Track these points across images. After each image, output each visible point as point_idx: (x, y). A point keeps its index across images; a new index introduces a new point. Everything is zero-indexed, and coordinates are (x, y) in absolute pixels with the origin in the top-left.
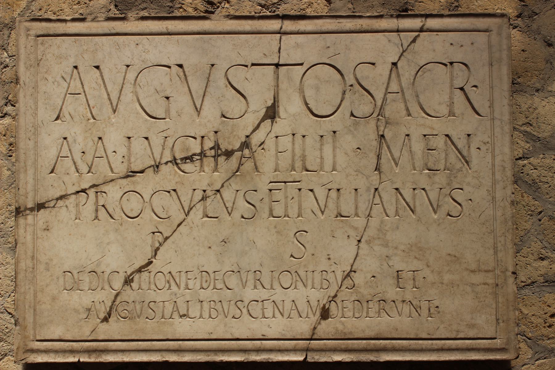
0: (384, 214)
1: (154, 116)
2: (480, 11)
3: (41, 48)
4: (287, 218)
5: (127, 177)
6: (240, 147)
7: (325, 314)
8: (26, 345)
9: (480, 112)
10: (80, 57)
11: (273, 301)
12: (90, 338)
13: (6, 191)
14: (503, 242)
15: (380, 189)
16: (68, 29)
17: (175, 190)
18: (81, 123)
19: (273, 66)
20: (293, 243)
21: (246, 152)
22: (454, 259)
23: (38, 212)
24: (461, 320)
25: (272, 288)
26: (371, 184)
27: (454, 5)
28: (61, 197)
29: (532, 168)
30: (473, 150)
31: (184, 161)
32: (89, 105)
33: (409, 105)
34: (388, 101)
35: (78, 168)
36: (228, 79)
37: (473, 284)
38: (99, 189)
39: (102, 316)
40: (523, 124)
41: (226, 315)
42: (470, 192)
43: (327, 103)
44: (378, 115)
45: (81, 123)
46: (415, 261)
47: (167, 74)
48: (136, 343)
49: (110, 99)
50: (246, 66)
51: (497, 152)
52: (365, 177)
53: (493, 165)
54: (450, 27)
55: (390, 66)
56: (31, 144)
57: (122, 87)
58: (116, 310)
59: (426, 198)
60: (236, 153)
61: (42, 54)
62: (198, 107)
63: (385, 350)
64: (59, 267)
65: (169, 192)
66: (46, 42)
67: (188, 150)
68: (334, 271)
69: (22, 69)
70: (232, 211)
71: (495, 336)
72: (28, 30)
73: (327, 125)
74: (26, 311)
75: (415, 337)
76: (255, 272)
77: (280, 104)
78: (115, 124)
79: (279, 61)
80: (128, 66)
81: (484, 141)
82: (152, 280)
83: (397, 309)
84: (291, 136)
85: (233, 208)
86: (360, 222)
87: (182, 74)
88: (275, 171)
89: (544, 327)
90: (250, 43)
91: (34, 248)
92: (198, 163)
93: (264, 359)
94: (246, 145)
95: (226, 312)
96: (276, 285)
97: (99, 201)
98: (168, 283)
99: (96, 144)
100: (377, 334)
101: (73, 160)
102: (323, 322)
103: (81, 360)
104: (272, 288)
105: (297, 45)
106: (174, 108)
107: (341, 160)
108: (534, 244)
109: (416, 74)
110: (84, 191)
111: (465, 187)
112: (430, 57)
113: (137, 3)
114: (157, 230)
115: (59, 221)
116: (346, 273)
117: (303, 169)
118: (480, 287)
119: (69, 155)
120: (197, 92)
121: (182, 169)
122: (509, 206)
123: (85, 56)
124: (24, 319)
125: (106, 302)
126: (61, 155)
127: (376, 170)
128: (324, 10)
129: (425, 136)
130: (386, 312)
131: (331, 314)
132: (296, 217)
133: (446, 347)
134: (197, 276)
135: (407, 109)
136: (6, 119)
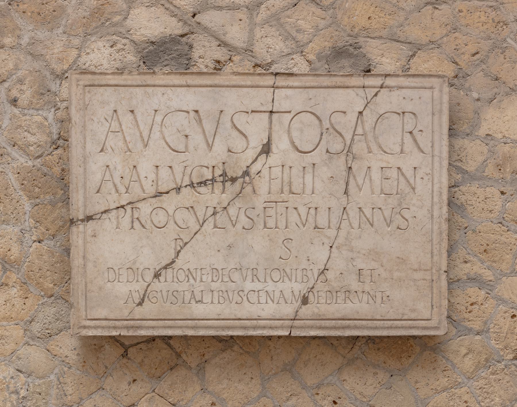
0: (350, 227)
1: (177, 150)
2: (426, 72)
3: (88, 96)
4: (277, 230)
5: (155, 196)
7: (305, 301)
9: (424, 151)
10: (119, 103)
11: (266, 291)
12: (128, 318)
14: (438, 249)
15: (347, 209)
17: (192, 207)
19: (268, 113)
20: (282, 248)
21: (247, 178)
22: (402, 261)
25: (265, 281)
26: (341, 204)
27: (406, 67)
28: (105, 212)
30: (418, 179)
31: (199, 185)
32: (126, 141)
33: (371, 144)
34: (355, 141)
35: (118, 189)
36: (233, 122)
37: (415, 280)
38: (134, 205)
39: (137, 301)
42: (414, 211)
44: (348, 152)
45: (120, 154)
47: (186, 118)
49: (141, 136)
50: (248, 113)
51: (436, 181)
52: (336, 199)
53: (433, 191)
55: (357, 114)
56: (81, 170)
57: (152, 127)
58: (148, 297)
61: (89, 100)
62: (211, 143)
63: (348, 327)
64: (104, 264)
65: (188, 208)
66: (92, 90)
67: (202, 176)
68: (312, 269)
69: (73, 111)
70: (236, 223)
71: (430, 318)
72: (78, 81)
73: (309, 159)
75: (371, 318)
76: (253, 269)
77: (273, 142)
78: (146, 156)
79: (273, 109)
80: (156, 111)
81: (427, 173)
82: (175, 275)
83: (358, 298)
84: (281, 167)
85: (236, 221)
86: (332, 233)
88: (269, 193)
89: (466, 312)
91: (85, 250)
92: (210, 187)
93: (259, 334)
94: (246, 173)
96: (268, 279)
99: (131, 171)
101: (114, 183)
102: (303, 307)
103: (122, 334)
104: (265, 281)
105: (287, 97)
107: (319, 185)
108: (461, 252)
110: (122, 207)
111: (411, 207)
113: (161, 61)
114: (179, 237)
115: (103, 229)
116: (321, 271)
117: (290, 192)
118: (420, 282)
119: (111, 179)
121: (198, 190)
123: (123, 102)
124: (78, 303)
125: (140, 291)
126: (104, 179)
129: (382, 168)
130: (350, 300)
131: (309, 301)
132: (284, 228)
133: (394, 326)
135: (369, 148)
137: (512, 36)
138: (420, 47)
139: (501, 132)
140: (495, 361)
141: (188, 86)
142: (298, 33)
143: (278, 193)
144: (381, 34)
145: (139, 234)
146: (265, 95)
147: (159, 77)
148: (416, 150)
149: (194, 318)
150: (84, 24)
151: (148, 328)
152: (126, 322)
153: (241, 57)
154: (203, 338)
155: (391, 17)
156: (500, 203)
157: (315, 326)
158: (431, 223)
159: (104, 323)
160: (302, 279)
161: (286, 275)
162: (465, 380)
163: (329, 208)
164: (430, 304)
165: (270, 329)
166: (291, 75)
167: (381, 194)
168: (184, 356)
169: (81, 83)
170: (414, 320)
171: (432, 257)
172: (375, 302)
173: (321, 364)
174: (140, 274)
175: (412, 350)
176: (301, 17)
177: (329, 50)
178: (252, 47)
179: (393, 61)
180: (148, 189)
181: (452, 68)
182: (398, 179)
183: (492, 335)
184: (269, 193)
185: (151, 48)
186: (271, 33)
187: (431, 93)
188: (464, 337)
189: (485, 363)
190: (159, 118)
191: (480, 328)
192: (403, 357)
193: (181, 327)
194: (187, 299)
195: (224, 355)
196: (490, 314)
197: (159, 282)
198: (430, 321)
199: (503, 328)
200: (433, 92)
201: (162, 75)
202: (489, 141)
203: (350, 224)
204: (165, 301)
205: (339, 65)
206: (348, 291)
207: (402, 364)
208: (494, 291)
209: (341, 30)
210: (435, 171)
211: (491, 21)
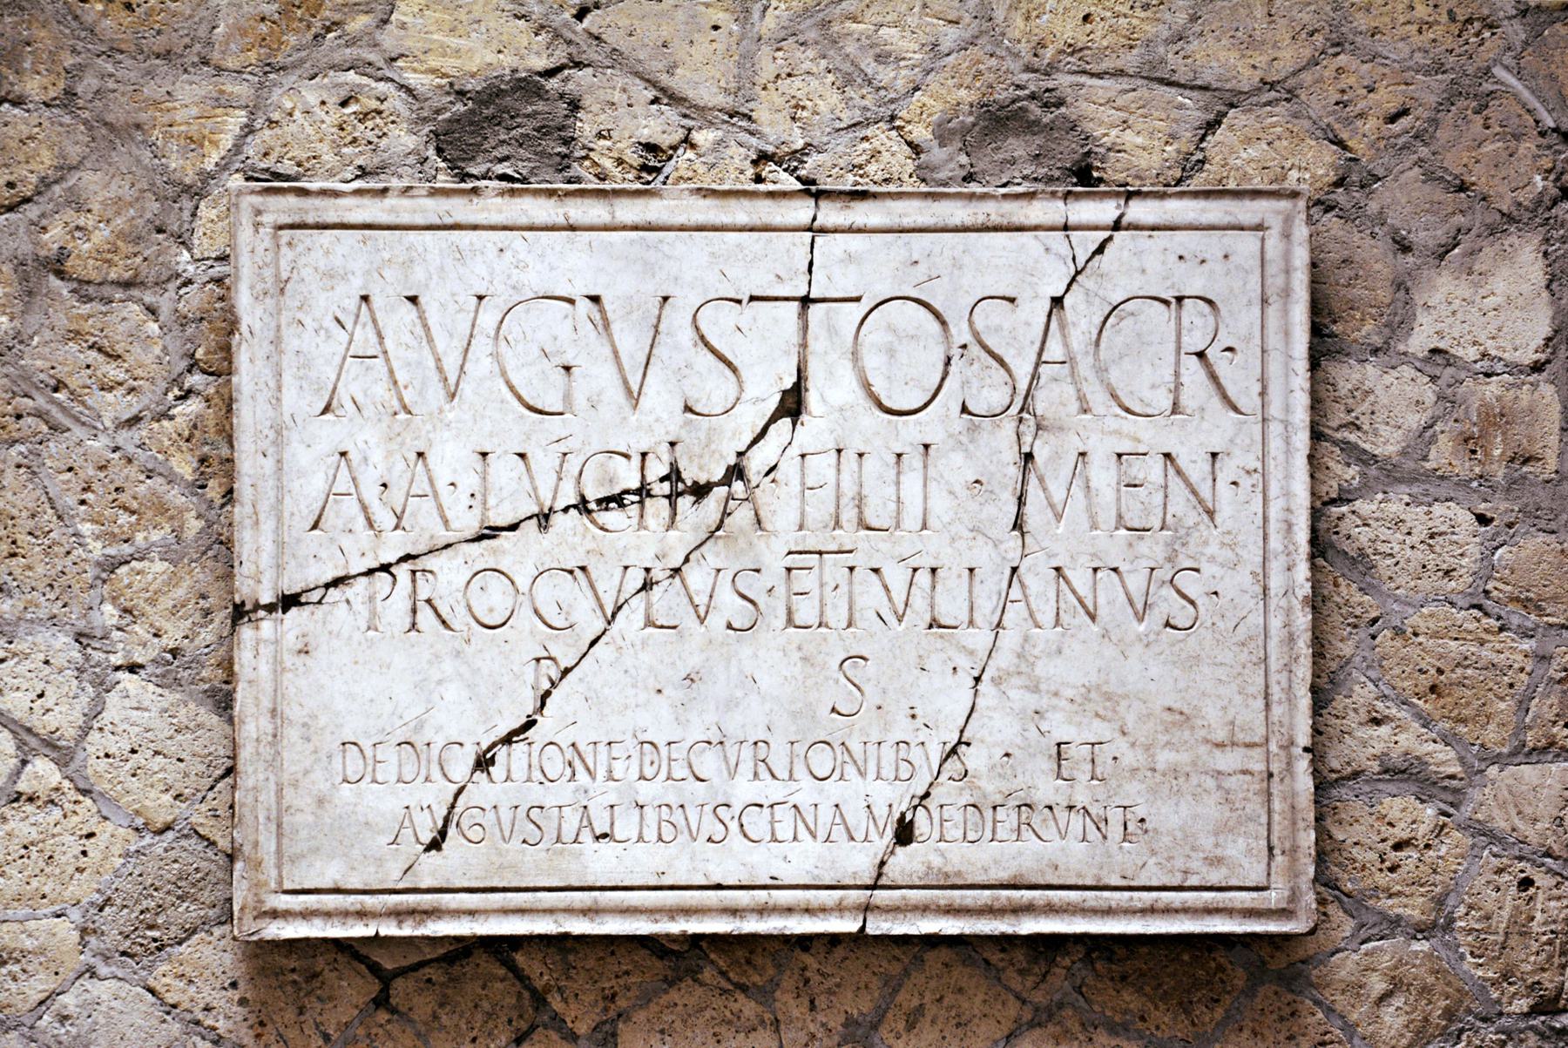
0: (1030, 622)
3: (287, 254)
5: (479, 538)
6: (725, 476)
7: (905, 833)
8: (260, 902)
9: (1239, 406)
10: (376, 275)
11: (795, 806)
12: (401, 886)
13: (193, 565)
14: (1285, 684)
15: (1022, 570)
16: (347, 213)
17: (583, 569)
18: (379, 420)
19: (796, 303)
20: (837, 681)
21: (738, 486)
22: (1181, 718)
23: (284, 612)
24: (1193, 849)
26: (1004, 558)
27: (1194, 158)
28: (337, 582)
29: (1359, 522)
31: (604, 505)
32: (395, 383)
33: (1085, 388)
34: (1042, 381)
35: (373, 518)
36: (697, 329)
37: (1219, 773)
38: (420, 564)
39: (427, 837)
40: (1341, 426)
41: (695, 834)
43: (912, 383)
44: (1022, 410)
45: (379, 420)
46: (1097, 723)
47: (566, 317)
48: (501, 895)
49: (440, 369)
50: (739, 302)
51: (1274, 490)
53: (1265, 519)
54: (1179, 219)
55: (1047, 305)
56: (269, 464)
57: (469, 344)
58: (457, 825)
59: (1121, 589)
60: (715, 489)
62: (635, 388)
63: (1029, 909)
64: (333, 733)
65: (571, 572)
70: (707, 612)
72: (259, 213)
73: (910, 431)
74: (261, 827)
75: (1094, 883)
76: (756, 743)
77: (810, 384)
78: (453, 425)
80: (481, 298)
82: (535, 762)
83: (1057, 824)
84: (834, 454)
85: (708, 607)
86: (980, 639)
87: (597, 317)
88: (801, 528)
89: (1381, 870)
90: (747, 252)
91: (275, 691)
92: (634, 510)
94: (736, 472)
95: (694, 829)
96: (800, 771)
97: (419, 591)
98: (570, 765)
100: (1015, 877)
102: (899, 849)
103: (383, 932)
105: (849, 257)
106: (582, 388)
107: (941, 506)
109: (1104, 322)
110: (385, 568)
111: (1204, 567)
113: (486, 146)
114: (546, 654)
115: (330, 633)
116: (948, 747)
118: (1233, 779)
119: (353, 490)
120: (632, 357)
121: (600, 522)
122: (1300, 607)
124: (256, 844)
125: (434, 807)
126: (334, 491)
127: (1014, 527)
128: (907, 168)
129: (1119, 456)
130: (1034, 830)
131: (917, 832)
133: (1160, 905)
134: (632, 752)
135: (1081, 398)
136: (189, 402)
137: (1508, 59)
138: (1235, 100)
139: (1475, 343)
140: (1475, 1017)
142: (880, 63)
143: (826, 527)
144: (1119, 64)
145: (432, 646)
146: (788, 251)
147: (489, 201)
148: (1216, 402)
149: (590, 884)
150: (264, 39)
153: (720, 133)
155: (1149, 14)
156: (1474, 550)
157: (933, 907)
158: (1262, 611)
160: (897, 770)
161: (849, 759)
163: (971, 570)
164: (1264, 843)
165: (807, 916)
167: (1117, 528)
168: (556, 1003)
169: (267, 219)
171: (1267, 706)
172: (1105, 837)
173: (954, 1022)
174: (435, 758)
175: (1222, 981)
176: (889, 18)
177: (971, 113)
178: (751, 105)
179: (1156, 143)
180: (458, 518)
181: (1328, 159)
182: (1166, 487)
183: (1461, 938)
184: (801, 528)
185: (459, 108)
186: (803, 66)
187: (1259, 244)
188: (1377, 943)
189: (1444, 1023)
191: (1424, 917)
192: (1199, 1000)
193: (550, 911)
195: (674, 995)
196: (1452, 875)
197: (492, 781)
198: (1265, 894)
199: (1495, 918)
200: (1263, 240)
201: (497, 195)
202: (1440, 368)
203: (1031, 615)
204: (507, 834)
205: (1000, 156)
206: (1026, 805)
207: (1193, 1024)
208: (1463, 809)
209: (1004, 54)
210: (1272, 463)
211: (1444, 18)
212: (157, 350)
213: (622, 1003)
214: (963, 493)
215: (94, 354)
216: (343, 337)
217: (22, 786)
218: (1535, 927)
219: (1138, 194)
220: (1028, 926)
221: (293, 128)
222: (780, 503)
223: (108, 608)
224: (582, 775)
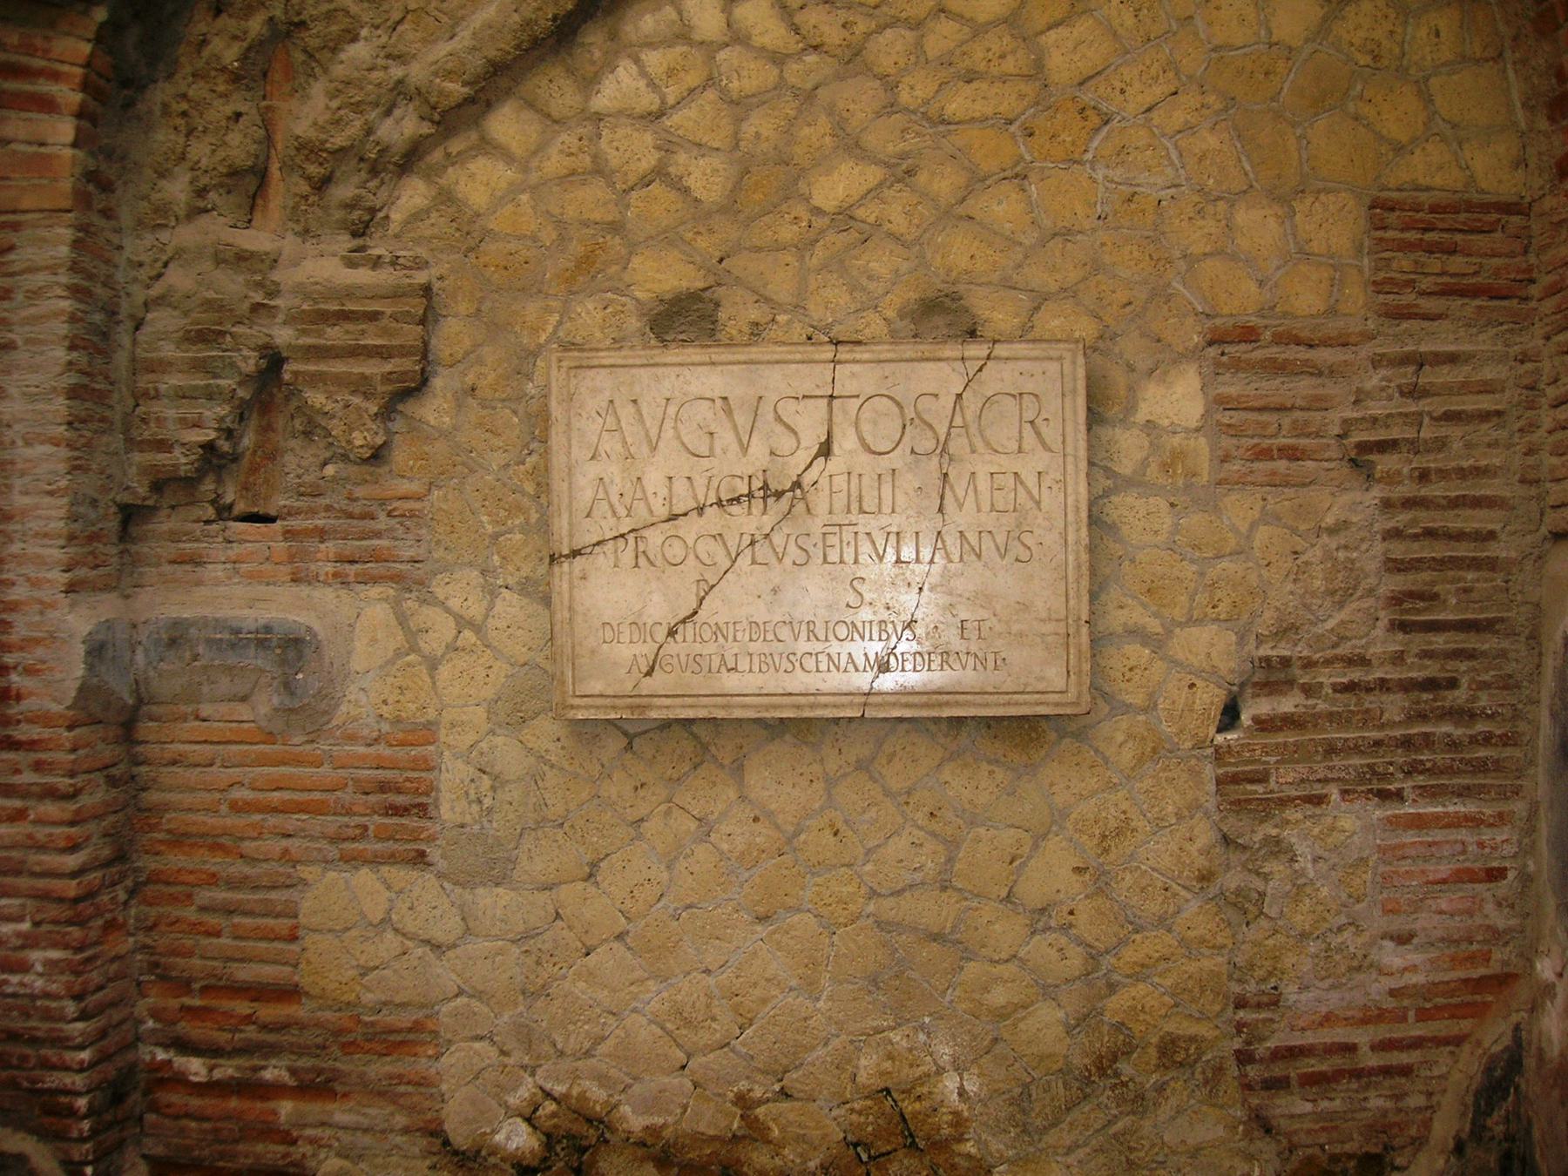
3: (574, 381)
5: (669, 520)
21: (798, 492)
22: (1024, 607)
28: (599, 543)
39: (645, 670)
46: (981, 610)
49: (647, 435)
56: (565, 485)
63: (947, 704)
67: (734, 490)
69: (553, 404)
73: (884, 463)
94: (797, 484)
101: (609, 502)
107: (901, 500)
110: (622, 536)
111: (1035, 530)
112: (998, 387)
124: (562, 673)
137: (1178, 279)
141: (713, 364)
148: (1040, 447)
151: (660, 707)
152: (630, 700)
154: (740, 721)
156: (1168, 521)
159: (599, 701)
162: (1124, 780)
164: (1065, 670)
166: (859, 343)
168: (713, 749)
169: (564, 364)
170: (1043, 693)
171: (1067, 601)
190: (672, 410)
194: (715, 665)
211: (1147, 258)
212: (517, 431)
213: (745, 750)
214: (912, 493)
215: (488, 434)
216: (600, 421)
217: (459, 643)
218: (1197, 707)
219: (999, 341)
220: (946, 713)
221: (581, 321)
222: (820, 503)
223: (496, 557)
224: (721, 639)
